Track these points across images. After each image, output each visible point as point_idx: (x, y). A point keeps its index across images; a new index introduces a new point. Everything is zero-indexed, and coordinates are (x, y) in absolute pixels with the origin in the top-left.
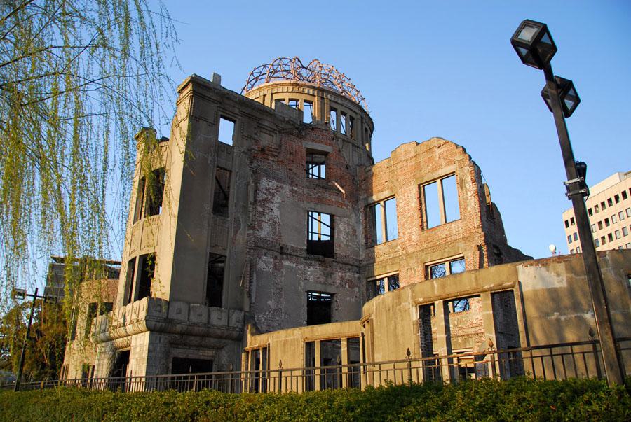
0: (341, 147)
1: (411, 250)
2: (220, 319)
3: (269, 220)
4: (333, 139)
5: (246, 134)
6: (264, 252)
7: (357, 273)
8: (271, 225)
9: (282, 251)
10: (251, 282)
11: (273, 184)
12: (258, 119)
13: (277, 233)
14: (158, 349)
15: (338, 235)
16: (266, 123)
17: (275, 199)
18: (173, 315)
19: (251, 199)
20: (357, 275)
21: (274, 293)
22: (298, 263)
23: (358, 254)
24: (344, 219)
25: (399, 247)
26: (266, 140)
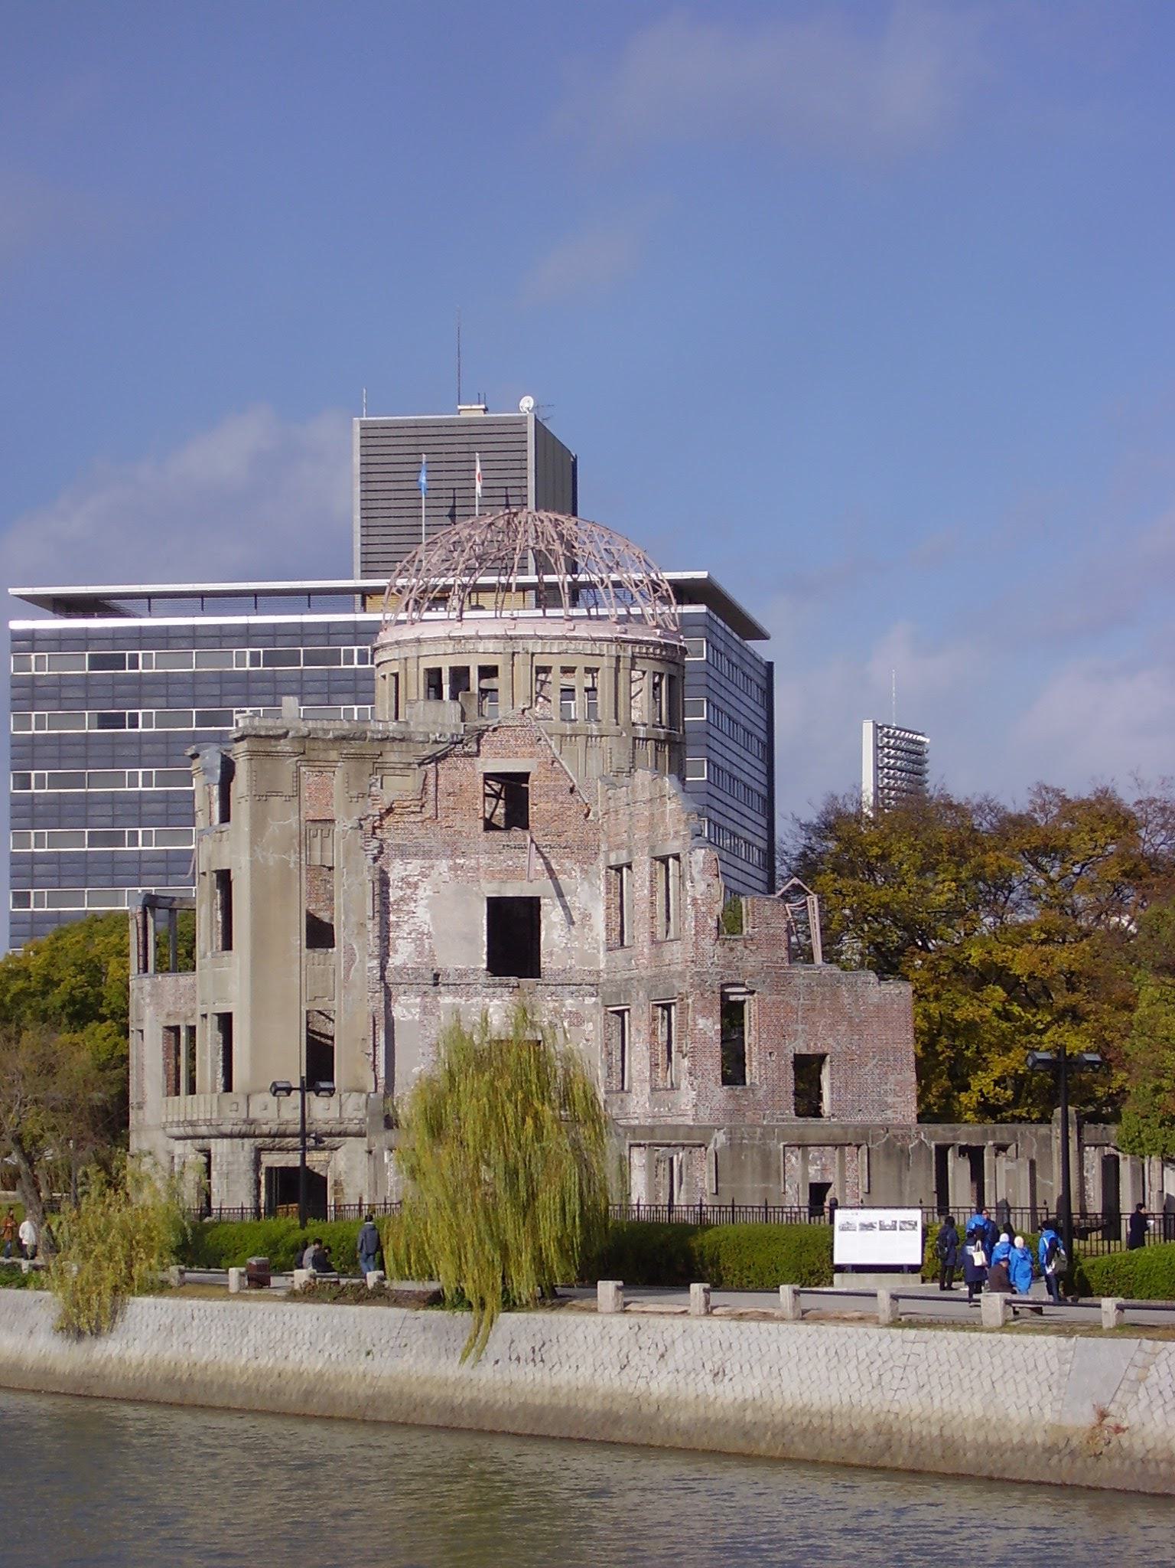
0: (557, 752)
3: (410, 934)
5: (354, 793)
6: (401, 988)
7: (592, 995)
11: (415, 866)
13: (426, 954)
14: (241, 1159)
17: (420, 892)
18: (256, 1113)
21: (423, 1054)
22: (469, 996)
23: (594, 959)
26: (398, 787)
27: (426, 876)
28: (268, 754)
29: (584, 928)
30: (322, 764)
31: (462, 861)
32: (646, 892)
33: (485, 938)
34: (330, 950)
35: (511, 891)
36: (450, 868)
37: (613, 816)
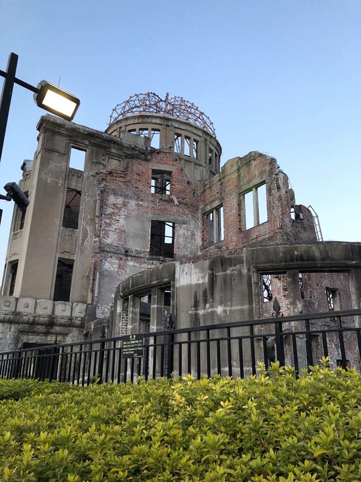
2: (64, 311)
3: (115, 230)
4: (176, 160)
5: (94, 160)
9: (127, 253)
10: (94, 280)
11: (120, 200)
12: (106, 148)
14: (8, 336)
15: (177, 239)
16: (114, 151)
17: (122, 212)
18: (21, 309)
19: (97, 214)
24: (184, 226)
25: (224, 247)
27: (125, 206)
29: (192, 238)
30: (81, 144)
31: (141, 203)
33: (150, 238)
34: (76, 230)
36: (136, 205)
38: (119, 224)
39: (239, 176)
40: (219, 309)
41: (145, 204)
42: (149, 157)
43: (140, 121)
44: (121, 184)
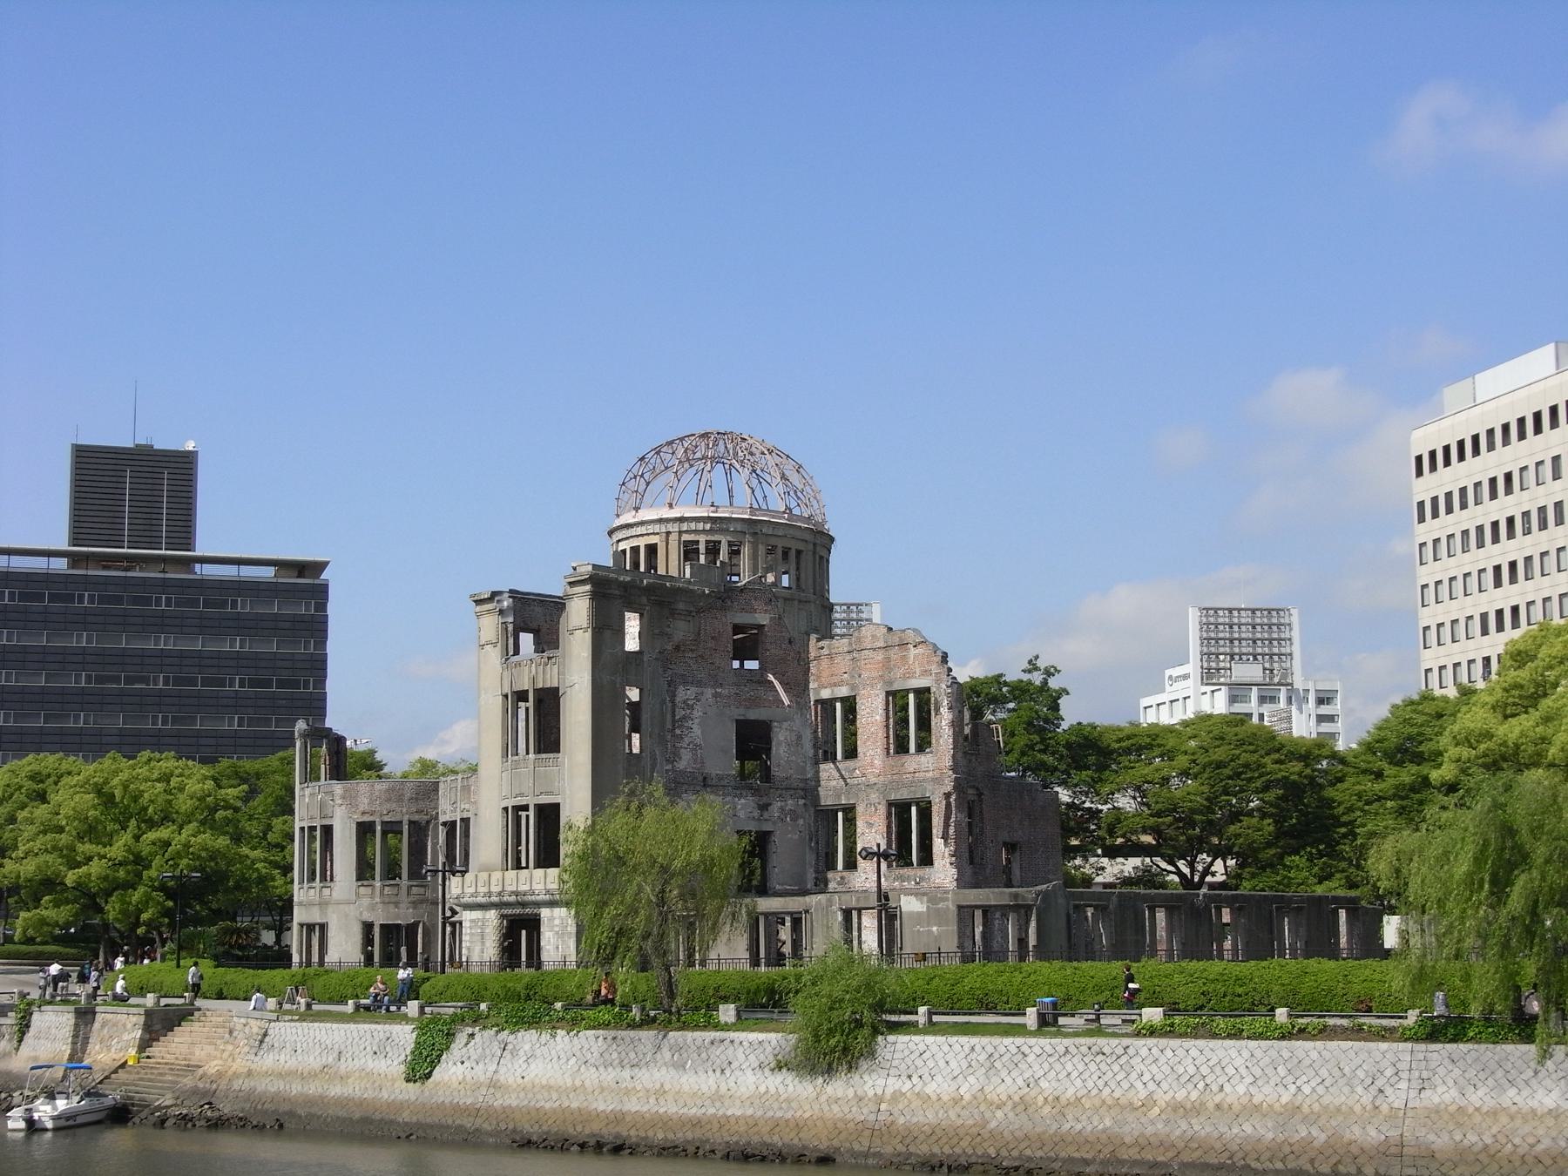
1: (873, 780)
5: (657, 631)
8: (692, 750)
16: (681, 606)
17: (695, 712)
20: (801, 802)
23: (804, 768)
24: (785, 725)
26: (681, 630)
28: (604, 596)
32: (878, 717)
33: (734, 751)
35: (753, 715)
37: (825, 663)
38: (692, 734)
39: (888, 659)
40: (935, 929)
41: (726, 692)
42: (729, 603)
43: (708, 526)
44: (691, 662)
